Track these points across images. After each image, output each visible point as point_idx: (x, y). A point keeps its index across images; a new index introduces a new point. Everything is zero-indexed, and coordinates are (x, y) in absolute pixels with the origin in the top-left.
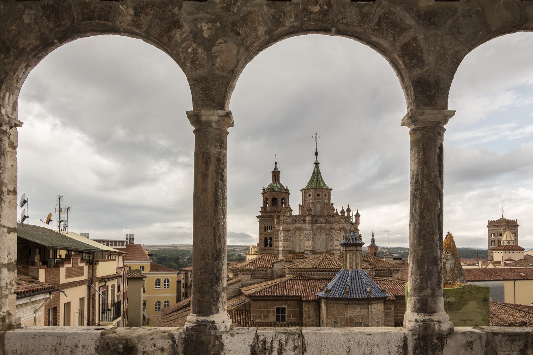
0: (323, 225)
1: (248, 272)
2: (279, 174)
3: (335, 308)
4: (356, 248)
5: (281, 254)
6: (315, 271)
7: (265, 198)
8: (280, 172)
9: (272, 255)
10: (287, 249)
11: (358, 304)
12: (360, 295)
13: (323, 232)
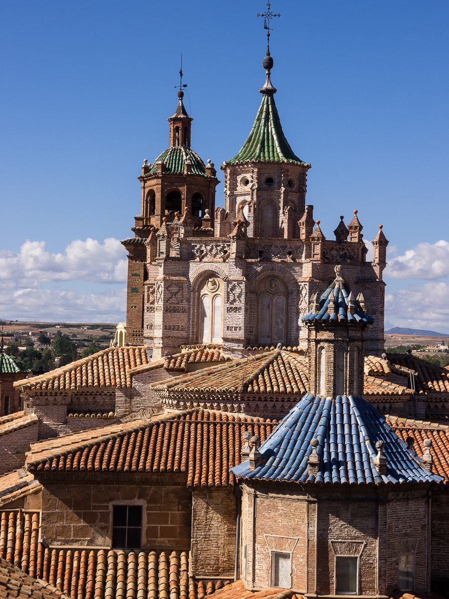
1: (59, 398)
2: (190, 124)
3: (277, 510)
5: (158, 348)
7: (147, 190)
8: (191, 119)
9: (134, 350)
10: (175, 333)
12: (351, 474)
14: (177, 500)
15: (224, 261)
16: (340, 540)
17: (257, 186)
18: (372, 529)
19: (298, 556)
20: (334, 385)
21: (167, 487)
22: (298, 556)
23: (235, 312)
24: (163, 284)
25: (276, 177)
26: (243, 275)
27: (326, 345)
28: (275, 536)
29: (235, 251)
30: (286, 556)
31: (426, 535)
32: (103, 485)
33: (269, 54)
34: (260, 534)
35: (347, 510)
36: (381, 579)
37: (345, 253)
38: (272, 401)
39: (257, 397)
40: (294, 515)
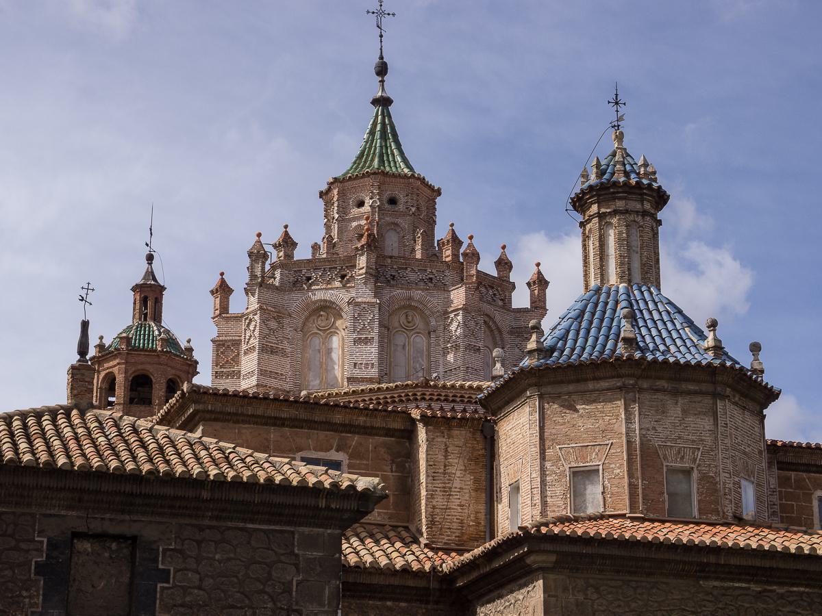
0: (417, 294)
4: (639, 206)
6: (424, 399)
7: (102, 374)
8: (163, 288)
11: (676, 393)
13: (418, 321)
14: (389, 457)
15: (344, 286)
16: (669, 444)
17: (379, 204)
18: (709, 431)
19: (613, 466)
20: (629, 269)
21: (376, 437)
22: (611, 466)
23: (366, 344)
24: (257, 317)
25: (401, 196)
26: (375, 297)
27: (614, 221)
28: (576, 445)
29: (365, 265)
30: (590, 473)
31: (763, 464)
32: (287, 429)
33: (382, 58)
34: (549, 448)
35: (676, 404)
36: (727, 499)
37: (495, 295)
38: (462, 401)
39: (443, 394)
40: (601, 412)
